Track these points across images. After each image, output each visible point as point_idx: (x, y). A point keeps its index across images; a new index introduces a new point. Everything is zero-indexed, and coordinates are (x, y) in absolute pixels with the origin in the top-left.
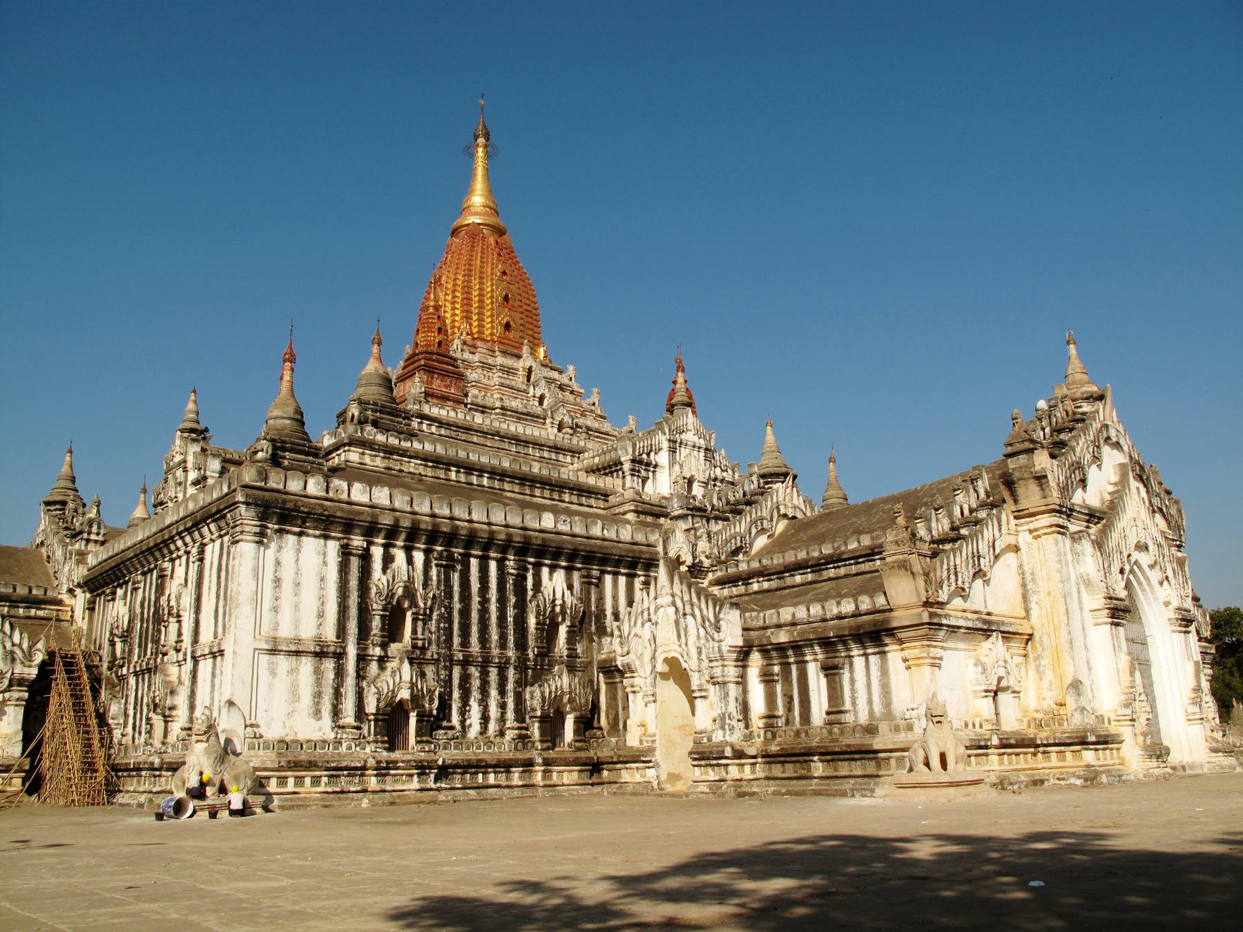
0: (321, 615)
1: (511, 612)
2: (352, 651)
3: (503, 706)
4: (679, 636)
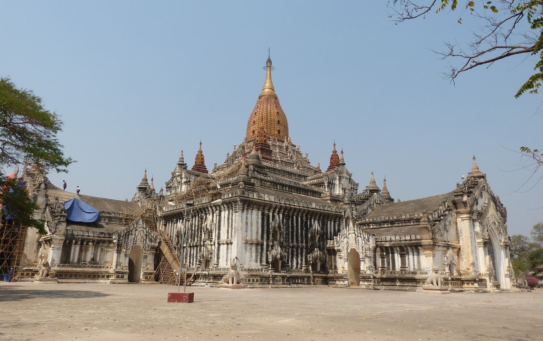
0: (257, 233)
1: (304, 232)
2: (265, 243)
3: (302, 260)
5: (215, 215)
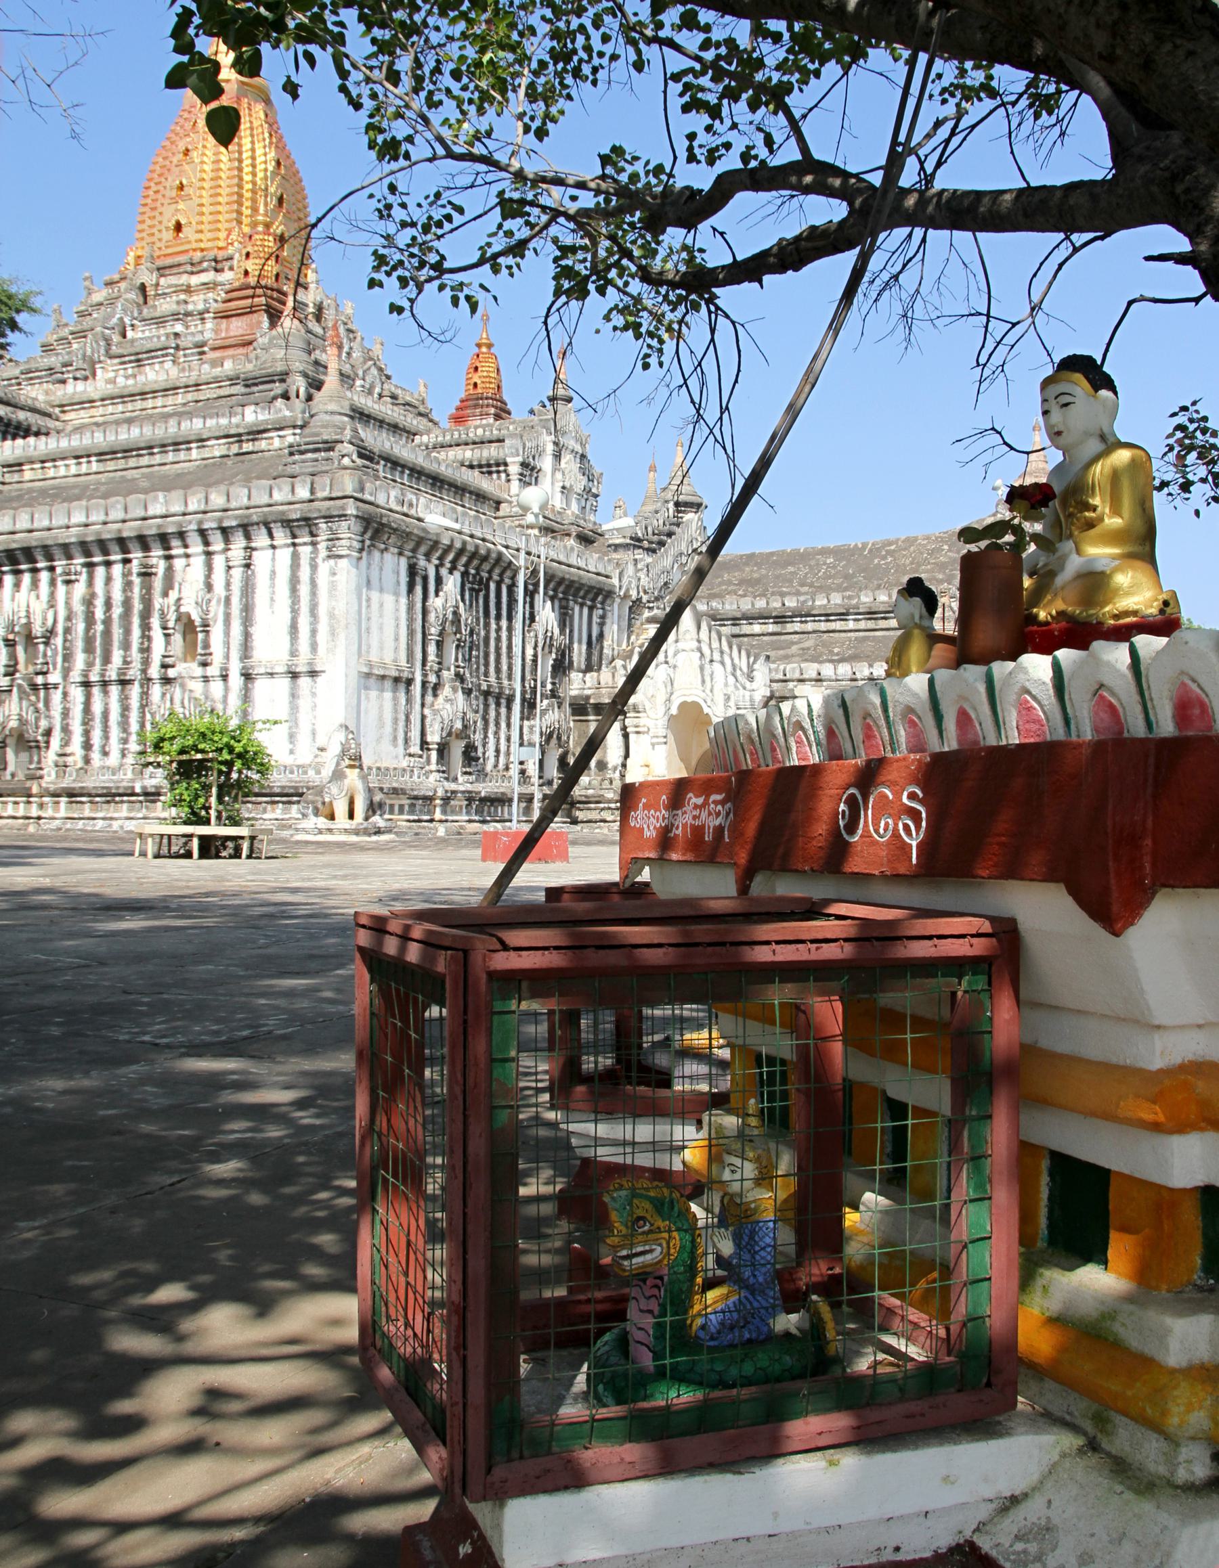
4: (703, 682)
5: (219, 562)
